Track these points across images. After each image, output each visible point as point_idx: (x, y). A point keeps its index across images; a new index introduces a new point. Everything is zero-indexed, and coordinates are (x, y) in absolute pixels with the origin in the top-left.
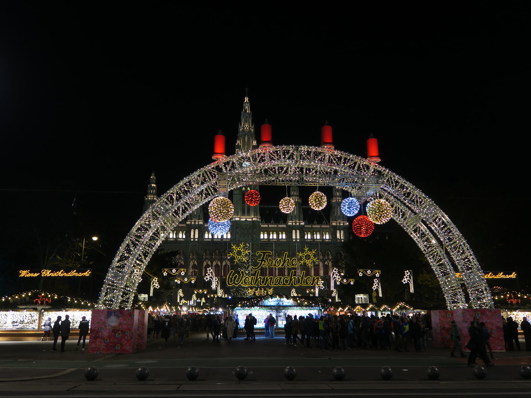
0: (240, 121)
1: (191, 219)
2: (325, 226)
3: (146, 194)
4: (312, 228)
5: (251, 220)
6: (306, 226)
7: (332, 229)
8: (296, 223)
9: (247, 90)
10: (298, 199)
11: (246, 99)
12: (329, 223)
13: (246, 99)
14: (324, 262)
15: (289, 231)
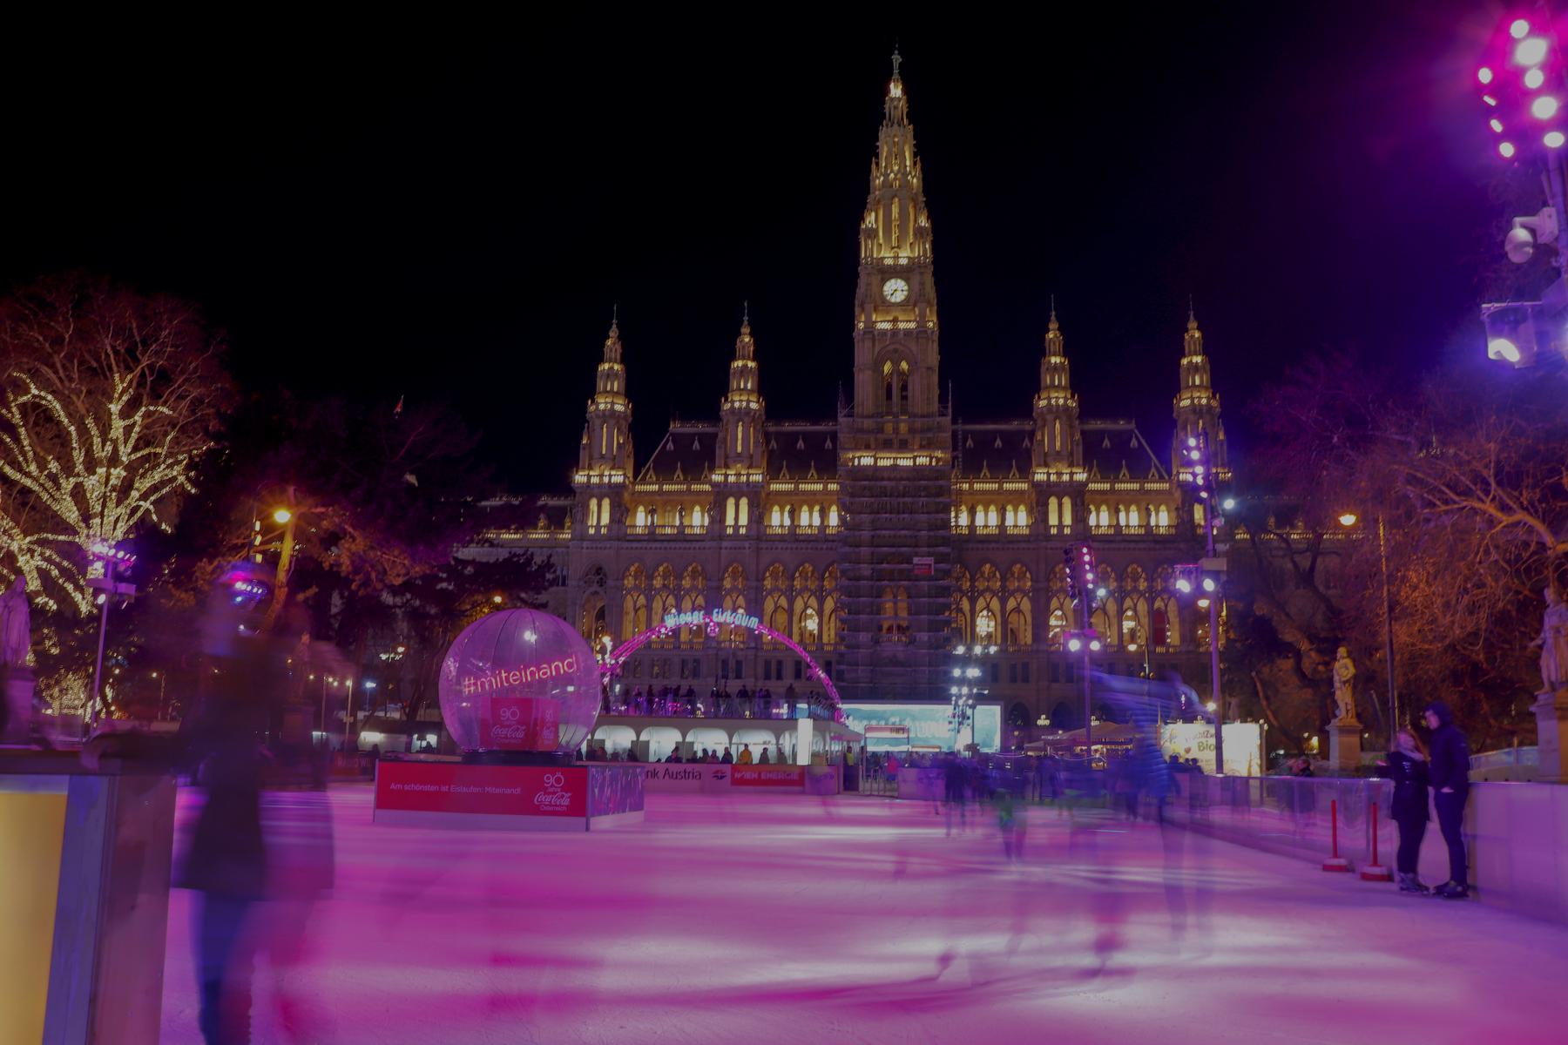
0: (877, 156)
1: (727, 466)
2: (1155, 486)
3: (591, 392)
4: (1112, 490)
5: (909, 463)
6: (1092, 486)
7: (1178, 494)
8: (1059, 474)
9: (897, 59)
10: (1066, 399)
11: (896, 91)
12: (1170, 473)
13: (896, 91)
14: (1151, 601)
15: (1039, 499)
